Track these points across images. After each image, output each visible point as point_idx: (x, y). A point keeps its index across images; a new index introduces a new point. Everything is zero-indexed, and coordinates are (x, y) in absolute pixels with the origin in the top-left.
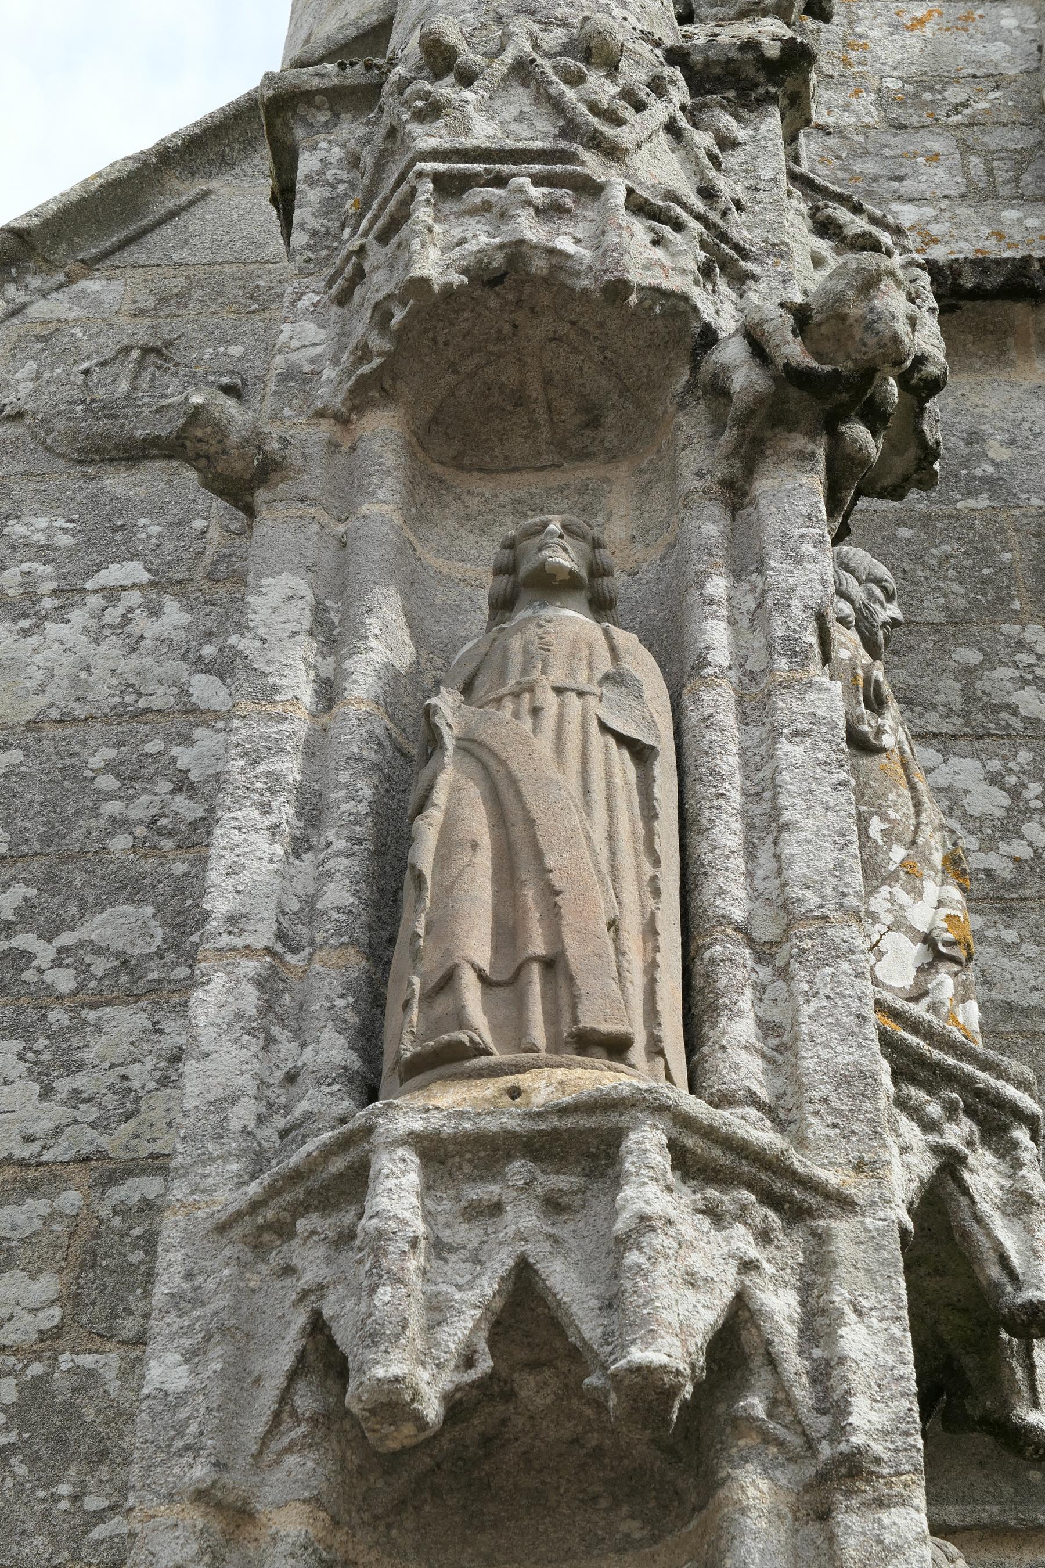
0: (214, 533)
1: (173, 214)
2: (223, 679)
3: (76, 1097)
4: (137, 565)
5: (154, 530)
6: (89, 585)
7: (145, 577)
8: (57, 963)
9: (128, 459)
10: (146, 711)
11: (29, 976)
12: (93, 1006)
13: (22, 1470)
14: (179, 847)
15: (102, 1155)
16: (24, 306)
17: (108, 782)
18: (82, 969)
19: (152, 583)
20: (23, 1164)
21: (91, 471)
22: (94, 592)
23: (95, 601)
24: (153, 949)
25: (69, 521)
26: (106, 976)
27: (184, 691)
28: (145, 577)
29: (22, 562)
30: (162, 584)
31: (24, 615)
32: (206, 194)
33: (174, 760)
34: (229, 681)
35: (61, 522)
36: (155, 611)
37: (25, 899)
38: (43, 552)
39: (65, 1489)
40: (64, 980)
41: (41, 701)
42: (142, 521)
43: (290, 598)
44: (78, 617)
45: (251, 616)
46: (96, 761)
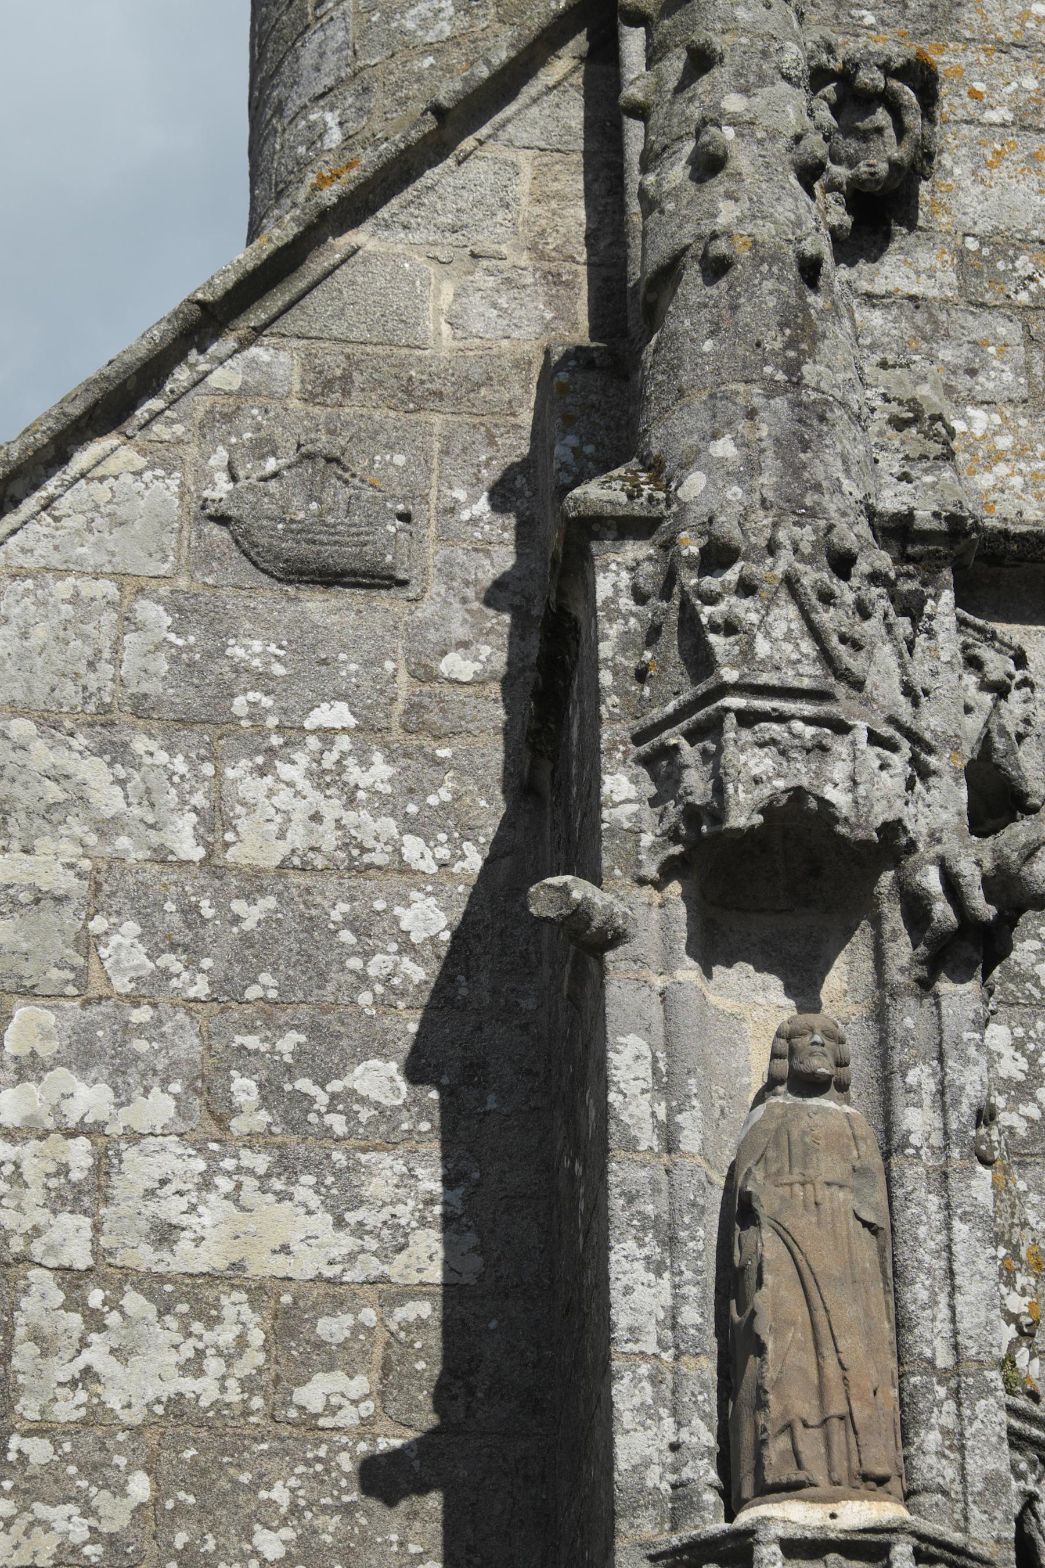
0: (403, 677)
1: (329, 273)
2: (427, 840)
3: (360, 1230)
4: (342, 707)
5: (353, 667)
6: (307, 725)
7: (351, 722)
8: (331, 1109)
9: (321, 583)
10: (370, 866)
11: (312, 1117)
12: (365, 1150)
13: (363, 1521)
14: (408, 1008)
15: (384, 1279)
16: (207, 374)
17: (347, 936)
18: (351, 1116)
19: (358, 729)
20: (328, 1281)
21: (291, 590)
22: (313, 732)
23: (313, 743)
24: (400, 1102)
25: (281, 647)
26: (369, 1123)
27: (398, 851)
28: (351, 722)
29: (246, 690)
30: (367, 730)
31: (257, 751)
32: (354, 251)
33: (396, 920)
34: (432, 844)
35: (273, 648)
36: (365, 764)
37: (299, 1044)
38: (262, 680)
39: (394, 1537)
40: (338, 1123)
41: (282, 849)
42: (343, 656)
43: (638, 1057)
44: (302, 758)
45: (614, 1072)
46: (336, 915)
